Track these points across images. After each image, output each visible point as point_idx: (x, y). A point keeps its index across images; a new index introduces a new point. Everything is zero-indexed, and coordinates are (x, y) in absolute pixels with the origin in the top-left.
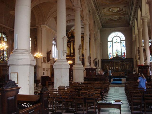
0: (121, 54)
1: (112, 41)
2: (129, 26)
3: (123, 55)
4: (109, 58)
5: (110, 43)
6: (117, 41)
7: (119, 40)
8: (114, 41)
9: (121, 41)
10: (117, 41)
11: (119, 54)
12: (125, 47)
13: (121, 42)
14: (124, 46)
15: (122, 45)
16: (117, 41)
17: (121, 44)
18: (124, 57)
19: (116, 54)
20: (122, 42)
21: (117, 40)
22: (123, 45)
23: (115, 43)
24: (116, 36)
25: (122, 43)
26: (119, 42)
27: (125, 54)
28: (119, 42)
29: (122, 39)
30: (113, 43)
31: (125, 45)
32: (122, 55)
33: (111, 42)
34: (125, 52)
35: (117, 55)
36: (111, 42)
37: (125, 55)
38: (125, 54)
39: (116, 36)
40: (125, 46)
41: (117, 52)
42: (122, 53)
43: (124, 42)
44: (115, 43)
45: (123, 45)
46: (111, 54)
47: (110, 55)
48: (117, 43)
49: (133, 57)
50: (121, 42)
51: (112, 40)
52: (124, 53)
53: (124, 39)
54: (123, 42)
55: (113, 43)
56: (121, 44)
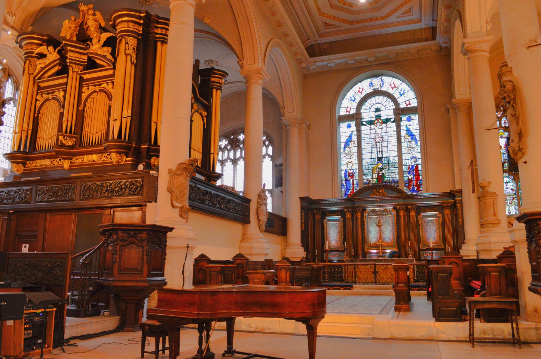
0: (401, 172)
1: (357, 117)
2: (434, 38)
3: (410, 181)
4: (343, 193)
5: (349, 126)
6: (377, 114)
7: (388, 111)
8: (367, 114)
9: (400, 112)
10: (378, 117)
11: (392, 175)
12: (419, 143)
13: (398, 121)
14: (412, 136)
15: (403, 133)
16: (378, 117)
17: (398, 127)
18: (413, 190)
19: (375, 176)
20: (404, 118)
21: (377, 110)
22: (408, 130)
23: (371, 123)
24: (376, 93)
25: (404, 122)
26: (387, 121)
27: (420, 172)
28: (387, 121)
29: (403, 106)
30: (359, 124)
31: (416, 132)
32: (406, 179)
33: (353, 123)
34: (419, 162)
35: (380, 178)
36: (353, 123)
37: (418, 179)
38: (418, 174)
39: (376, 93)
40: (418, 138)
41: (380, 166)
42: (405, 169)
43: (415, 118)
44: (371, 123)
45: (408, 130)
46: (352, 175)
47: (346, 180)
48: (379, 129)
49: (458, 187)
50: (398, 121)
51: (353, 111)
52: (414, 170)
53: (414, 103)
54: (409, 120)
55: (359, 124)
56: (398, 127)
